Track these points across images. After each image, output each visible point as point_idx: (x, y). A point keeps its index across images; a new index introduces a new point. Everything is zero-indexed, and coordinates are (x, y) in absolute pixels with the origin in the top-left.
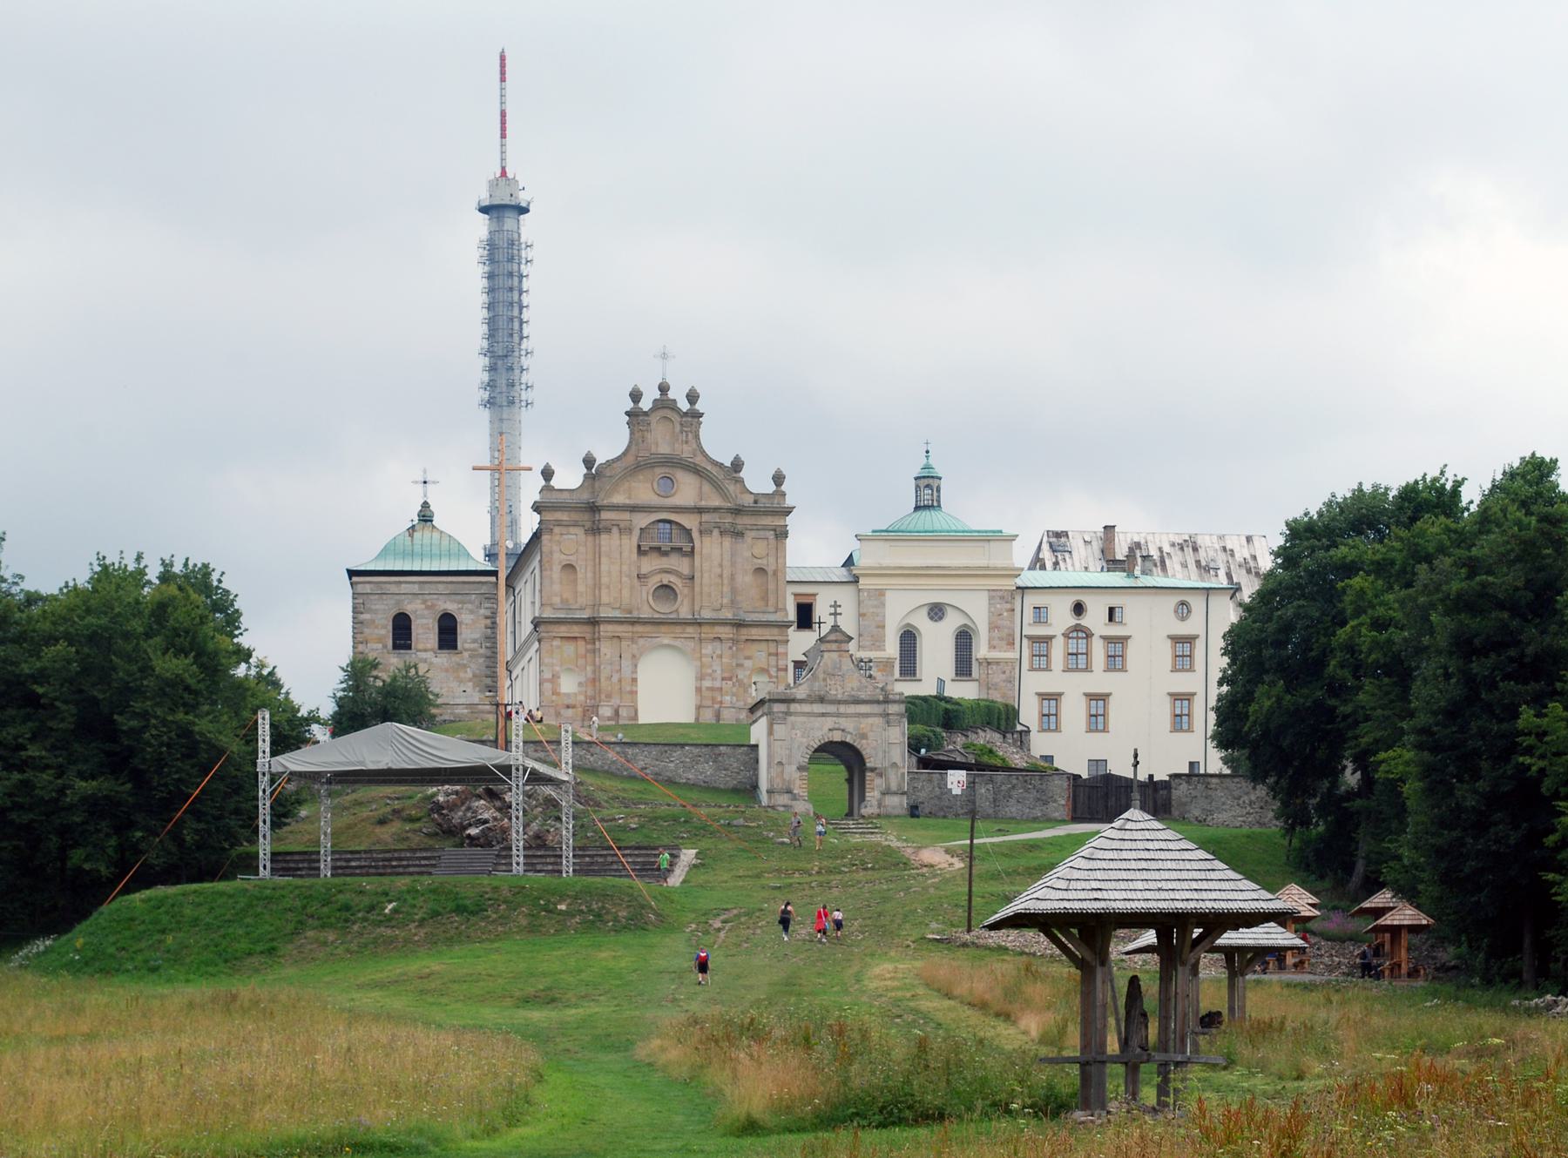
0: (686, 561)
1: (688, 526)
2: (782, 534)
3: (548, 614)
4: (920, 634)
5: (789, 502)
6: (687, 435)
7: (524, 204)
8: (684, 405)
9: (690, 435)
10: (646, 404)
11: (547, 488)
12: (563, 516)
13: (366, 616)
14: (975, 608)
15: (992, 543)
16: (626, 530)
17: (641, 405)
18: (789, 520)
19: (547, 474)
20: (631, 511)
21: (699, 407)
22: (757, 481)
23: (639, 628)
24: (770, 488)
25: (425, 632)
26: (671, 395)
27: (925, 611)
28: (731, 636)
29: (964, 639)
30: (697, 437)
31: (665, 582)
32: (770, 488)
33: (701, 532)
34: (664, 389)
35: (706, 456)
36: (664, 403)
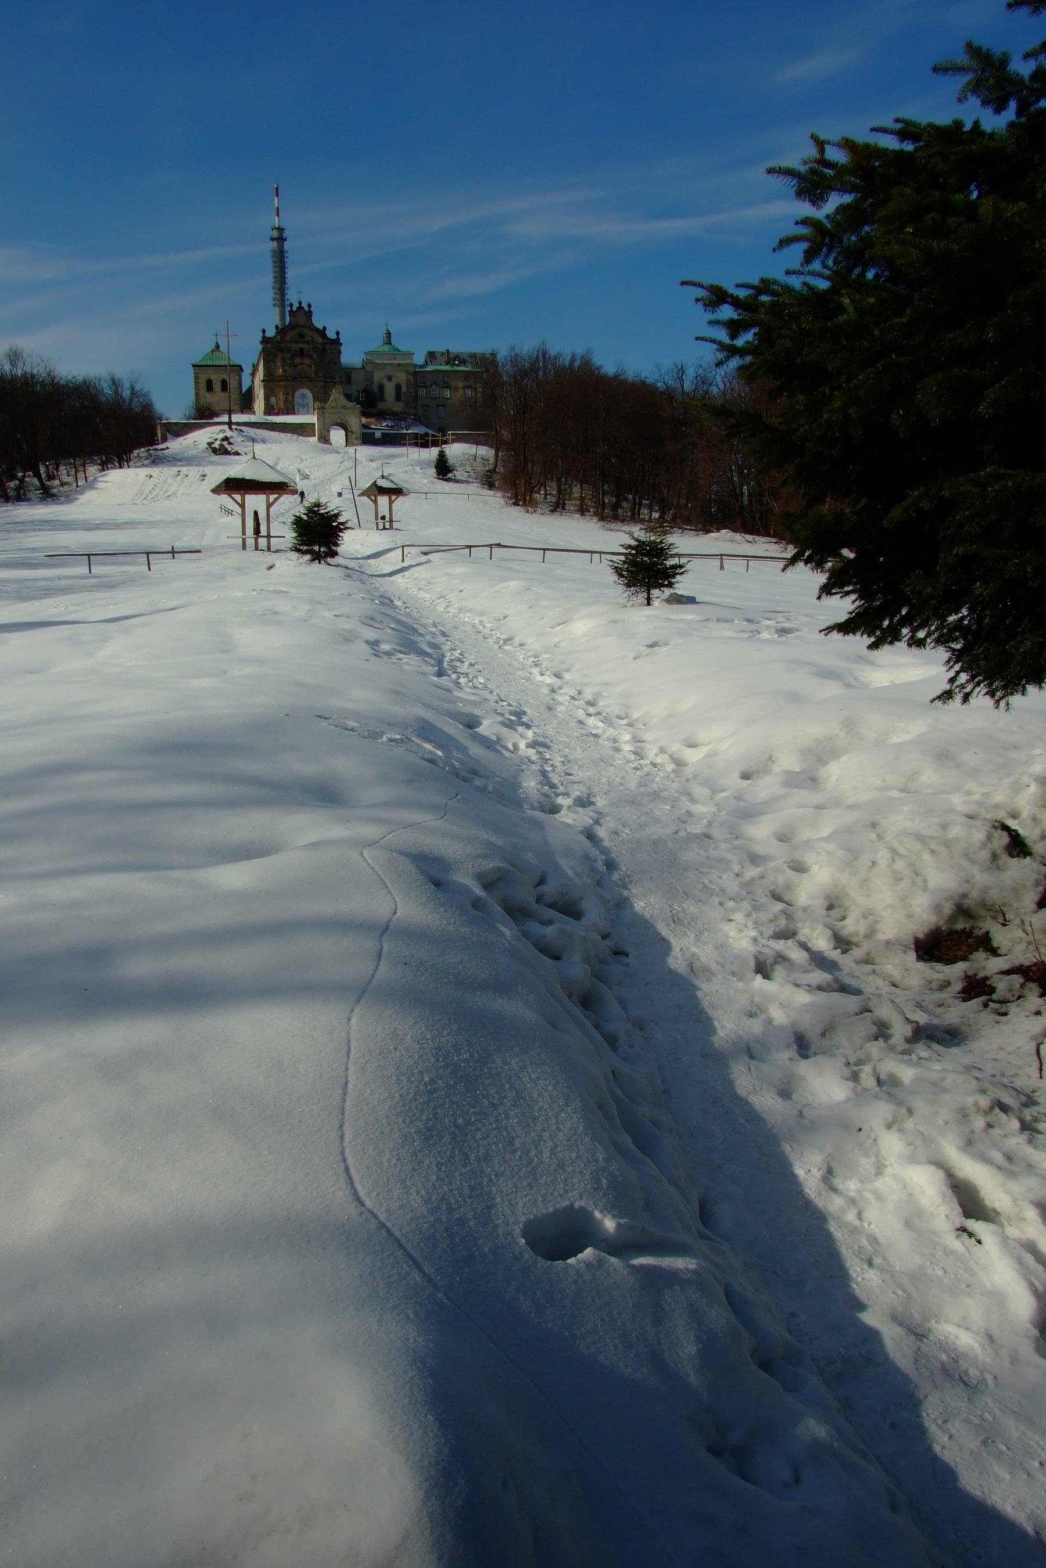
2: (340, 352)
3: (265, 378)
7: (284, 237)
8: (306, 309)
11: (264, 337)
12: (269, 346)
13: (199, 381)
14: (401, 377)
16: (289, 350)
19: (264, 331)
22: (331, 335)
23: (294, 383)
24: (334, 337)
25: (217, 386)
26: (302, 305)
27: (386, 379)
29: (398, 388)
33: (313, 352)
34: (300, 303)
36: (300, 308)
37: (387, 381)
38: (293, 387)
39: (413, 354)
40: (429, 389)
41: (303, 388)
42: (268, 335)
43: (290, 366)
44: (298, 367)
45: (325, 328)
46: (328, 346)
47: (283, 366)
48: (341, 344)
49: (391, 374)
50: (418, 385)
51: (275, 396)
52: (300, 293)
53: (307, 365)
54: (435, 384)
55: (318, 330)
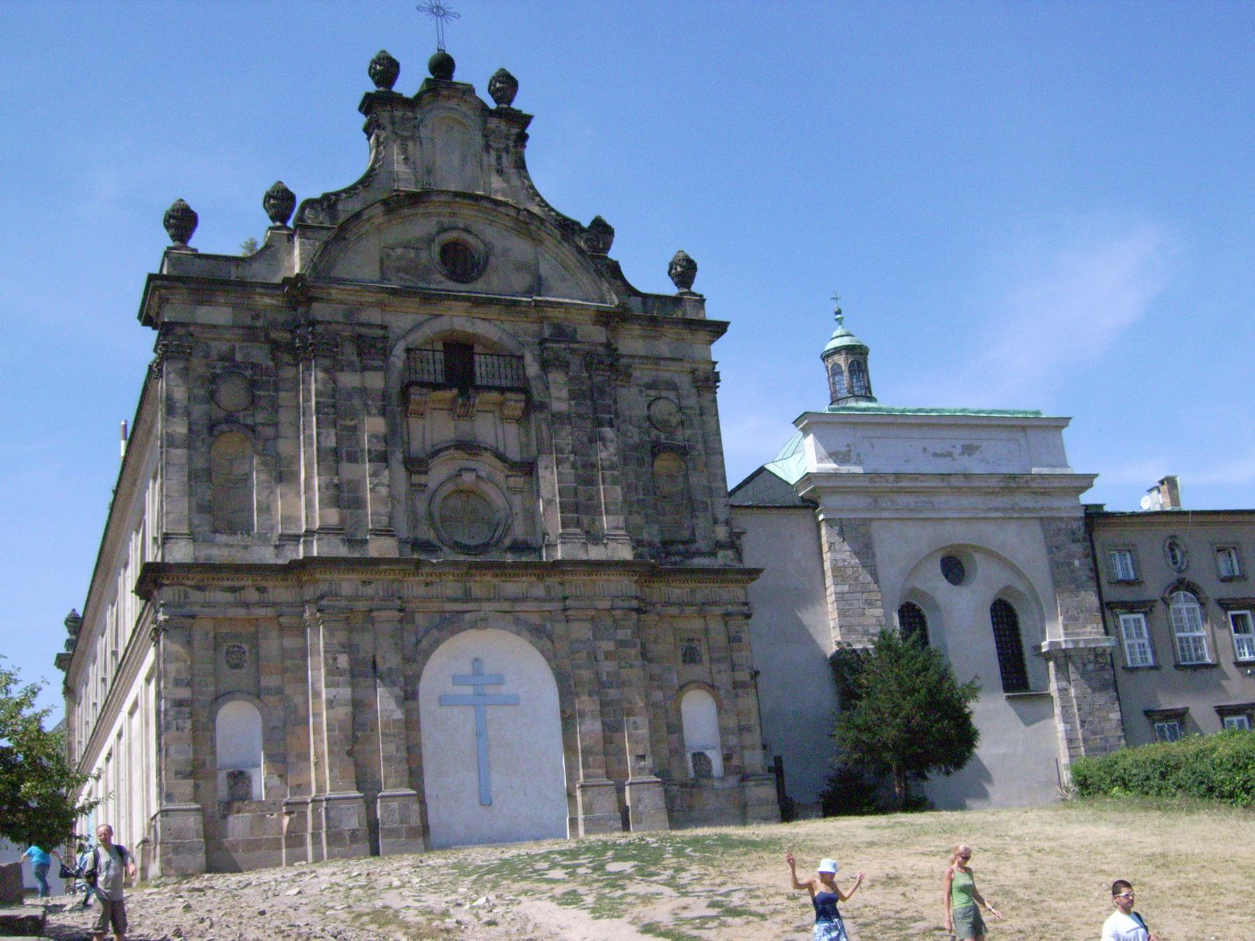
0: (512, 429)
1: (510, 344)
2: (708, 381)
4: (936, 607)
5: (712, 312)
6: (499, 158)
9: (504, 155)
10: (409, 84)
12: (217, 314)
15: (1030, 433)
17: (398, 88)
18: (720, 351)
20: (382, 306)
21: (520, 103)
23: (414, 587)
24: (671, 290)
26: (458, 77)
28: (635, 603)
30: (521, 165)
31: (468, 478)
32: (671, 290)
33: (545, 365)
34: (443, 66)
35: (543, 204)
37: (944, 583)
38: (406, 617)
39: (1060, 424)
40: (1159, 607)
41: (481, 623)
42: (204, 241)
43: (382, 458)
44: (439, 472)
45: (602, 231)
46: (632, 343)
47: (333, 458)
48: (719, 328)
49: (956, 534)
50: (1112, 594)
51: (256, 694)
52: (438, 12)
53: (501, 457)
54: (1192, 588)
55: (567, 227)
